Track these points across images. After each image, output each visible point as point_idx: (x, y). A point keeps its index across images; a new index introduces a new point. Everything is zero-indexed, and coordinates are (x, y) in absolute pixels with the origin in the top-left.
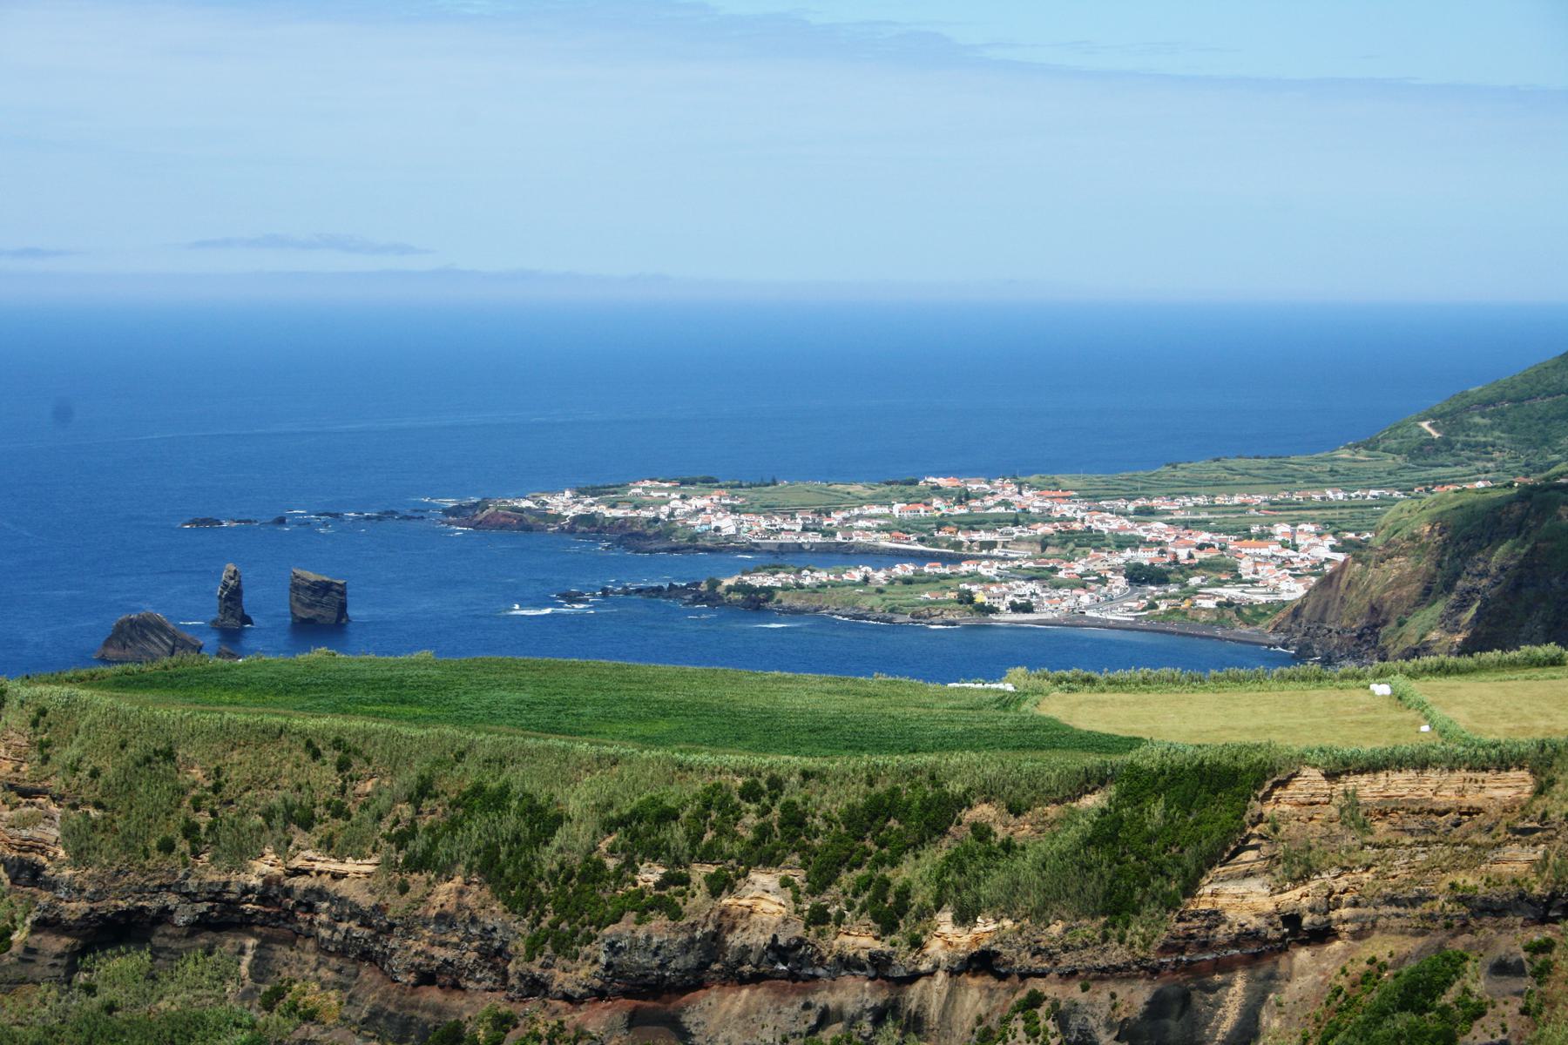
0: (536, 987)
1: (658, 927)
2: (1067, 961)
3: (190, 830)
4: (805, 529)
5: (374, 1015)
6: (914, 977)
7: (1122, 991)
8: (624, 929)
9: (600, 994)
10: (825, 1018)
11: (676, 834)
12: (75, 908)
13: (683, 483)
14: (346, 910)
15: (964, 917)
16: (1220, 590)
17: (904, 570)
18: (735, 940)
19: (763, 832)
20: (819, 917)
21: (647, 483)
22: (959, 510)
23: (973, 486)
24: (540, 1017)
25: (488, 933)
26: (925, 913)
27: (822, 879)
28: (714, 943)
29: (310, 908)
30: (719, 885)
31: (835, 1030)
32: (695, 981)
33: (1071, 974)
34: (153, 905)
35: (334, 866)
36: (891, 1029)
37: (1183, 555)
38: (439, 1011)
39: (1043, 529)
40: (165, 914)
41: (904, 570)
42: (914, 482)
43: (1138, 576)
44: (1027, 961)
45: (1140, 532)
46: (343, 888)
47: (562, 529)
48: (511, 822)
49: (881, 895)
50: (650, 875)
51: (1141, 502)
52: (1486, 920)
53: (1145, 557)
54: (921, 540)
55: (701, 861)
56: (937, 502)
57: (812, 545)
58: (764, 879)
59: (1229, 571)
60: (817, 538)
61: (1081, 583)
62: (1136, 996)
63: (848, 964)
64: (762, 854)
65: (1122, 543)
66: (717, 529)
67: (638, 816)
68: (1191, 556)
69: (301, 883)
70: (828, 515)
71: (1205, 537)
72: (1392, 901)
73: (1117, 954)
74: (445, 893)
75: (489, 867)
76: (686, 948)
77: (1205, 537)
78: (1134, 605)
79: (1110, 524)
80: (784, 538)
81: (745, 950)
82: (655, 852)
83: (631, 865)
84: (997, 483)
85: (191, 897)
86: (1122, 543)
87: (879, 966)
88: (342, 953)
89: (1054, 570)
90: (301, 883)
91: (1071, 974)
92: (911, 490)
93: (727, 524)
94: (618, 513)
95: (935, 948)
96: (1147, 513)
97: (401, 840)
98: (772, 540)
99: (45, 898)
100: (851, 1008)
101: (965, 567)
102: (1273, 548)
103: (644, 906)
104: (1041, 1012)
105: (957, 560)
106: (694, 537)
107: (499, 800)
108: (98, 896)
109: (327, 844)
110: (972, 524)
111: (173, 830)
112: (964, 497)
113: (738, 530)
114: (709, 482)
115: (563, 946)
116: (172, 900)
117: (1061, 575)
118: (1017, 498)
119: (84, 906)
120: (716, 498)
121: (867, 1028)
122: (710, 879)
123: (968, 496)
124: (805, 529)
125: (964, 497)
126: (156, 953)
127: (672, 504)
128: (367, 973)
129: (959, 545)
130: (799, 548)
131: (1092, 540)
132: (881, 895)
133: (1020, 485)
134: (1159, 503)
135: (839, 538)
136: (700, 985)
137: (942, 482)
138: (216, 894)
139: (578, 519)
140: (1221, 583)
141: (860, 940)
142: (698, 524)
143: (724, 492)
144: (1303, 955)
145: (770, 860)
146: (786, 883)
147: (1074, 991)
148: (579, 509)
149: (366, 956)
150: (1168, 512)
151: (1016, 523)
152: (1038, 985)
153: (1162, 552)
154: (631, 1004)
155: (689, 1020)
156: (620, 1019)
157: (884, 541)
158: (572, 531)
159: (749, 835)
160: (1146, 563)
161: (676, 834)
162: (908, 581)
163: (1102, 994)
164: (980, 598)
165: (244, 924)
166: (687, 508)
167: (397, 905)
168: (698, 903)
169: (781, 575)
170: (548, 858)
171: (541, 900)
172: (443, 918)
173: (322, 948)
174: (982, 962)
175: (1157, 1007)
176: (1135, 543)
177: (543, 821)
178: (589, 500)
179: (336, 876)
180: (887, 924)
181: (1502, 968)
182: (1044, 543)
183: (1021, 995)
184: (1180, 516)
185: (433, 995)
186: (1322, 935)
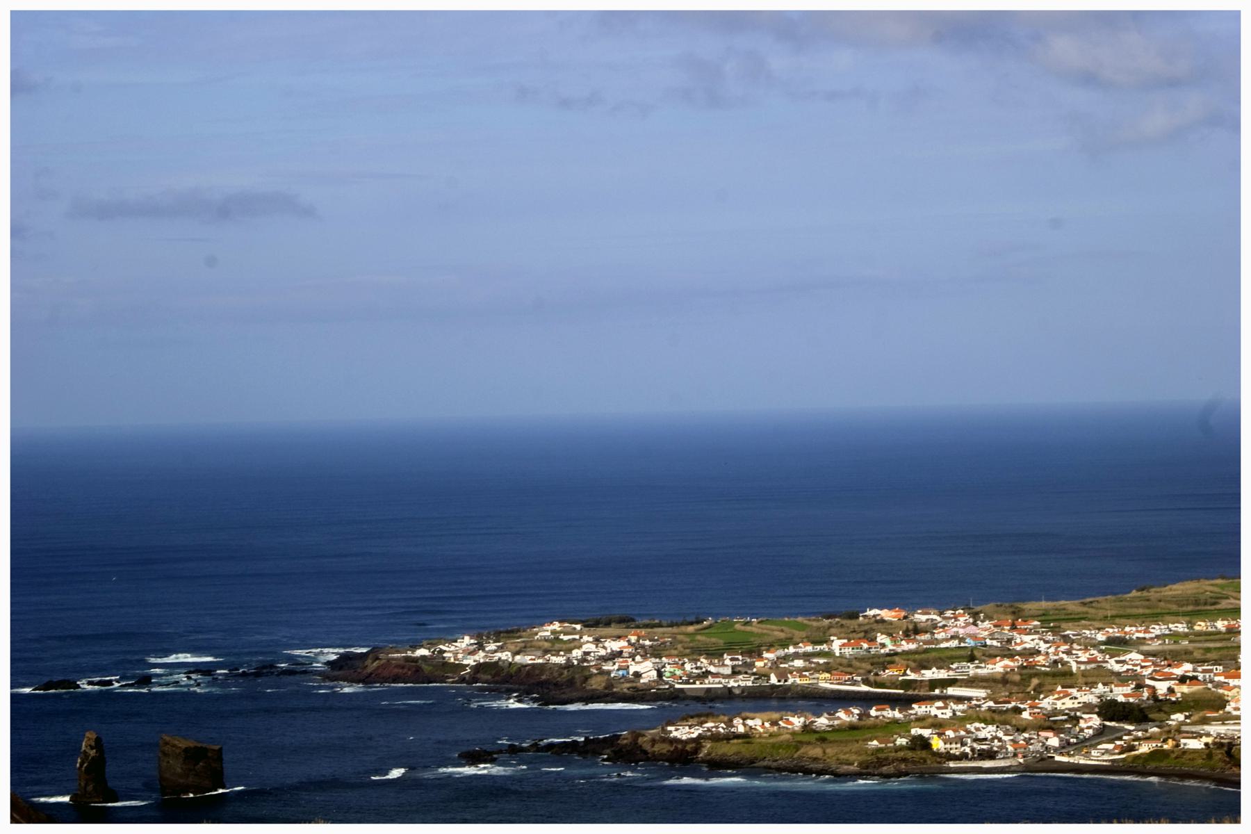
4: (735, 673)
13: (596, 624)
16: (1207, 728)
21: (556, 626)
22: (907, 646)
23: (920, 617)
37: (1162, 688)
42: (854, 616)
45: (1113, 665)
47: (463, 680)
51: (1113, 631)
54: (866, 682)
56: (881, 638)
57: (744, 689)
60: (745, 681)
66: (637, 675)
68: (1171, 690)
70: (760, 657)
71: (1187, 668)
77: (1187, 668)
78: (1111, 746)
80: (710, 683)
84: (949, 613)
89: (1018, 711)
92: (852, 624)
93: (646, 669)
94: (526, 659)
96: (1119, 645)
98: (698, 685)
101: (919, 709)
106: (610, 684)
110: (922, 660)
112: (913, 631)
113: (660, 674)
114: (626, 621)
117: (1025, 715)
118: (972, 629)
120: (633, 639)
123: (917, 630)
124: (735, 673)
125: (913, 631)
127: (586, 648)
129: (908, 684)
130: (728, 694)
131: (1061, 676)
133: (975, 615)
134: (1134, 632)
135: (774, 680)
137: (886, 614)
139: (479, 667)
140: (1205, 721)
143: (643, 632)
148: (480, 657)
150: (1141, 641)
151: (972, 659)
153: (1139, 686)
157: (826, 683)
158: (473, 678)
160: (1121, 699)
162: (852, 727)
166: (602, 652)
169: (710, 725)
178: (491, 646)
182: (1004, 680)
184: (1155, 646)
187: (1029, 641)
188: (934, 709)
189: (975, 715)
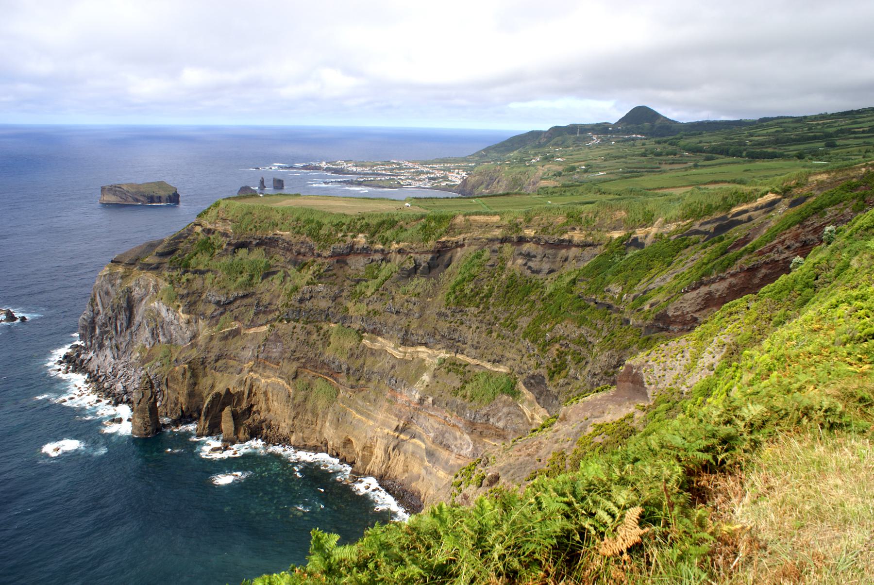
0: (319, 255)
1: (342, 245)
2: (416, 251)
3: (255, 227)
5: (290, 261)
6: (389, 253)
7: (426, 255)
8: (336, 245)
9: (332, 256)
10: (372, 261)
11: (345, 227)
12: (234, 242)
14: (284, 241)
15: (398, 243)
17: (387, 178)
18: (356, 247)
19: (362, 226)
20: (372, 242)
24: (320, 260)
25: (310, 246)
26: (391, 241)
27: (373, 235)
28: (352, 247)
29: (278, 241)
30: (354, 237)
31: (374, 263)
32: (348, 254)
33: (417, 253)
34: (249, 241)
35: (281, 233)
36: (384, 263)
38: (302, 260)
39: (413, 170)
40: (251, 242)
41: (387, 178)
43: (430, 179)
44: (409, 250)
46: (284, 237)
48: (314, 225)
49: (383, 239)
50: (340, 235)
52: (492, 242)
53: (432, 176)
55: (350, 232)
58: (361, 235)
59: (445, 178)
60: (371, 172)
61: (420, 180)
62: (430, 256)
63: (376, 251)
64: (361, 231)
65: (428, 173)
67: (337, 224)
69: (276, 236)
72: (475, 239)
73: (425, 249)
74: (302, 238)
75: (310, 234)
76: (347, 248)
79: (426, 170)
81: (358, 249)
82: (341, 231)
83: (337, 232)
85: (255, 239)
86: (428, 173)
87: (383, 250)
88: (284, 249)
90: (276, 236)
91: (417, 253)
93: (354, 169)
95: (393, 248)
97: (294, 228)
99: (228, 239)
100: (377, 259)
102: (455, 174)
103: (339, 241)
104: (412, 259)
105: (397, 176)
106: (348, 171)
107: (312, 221)
108: (238, 239)
109: (281, 230)
110: (400, 169)
111: (252, 227)
115: (324, 247)
116: (252, 240)
119: (236, 241)
121: (380, 262)
122: (352, 236)
126: (249, 249)
128: (288, 253)
131: (422, 172)
132: (383, 239)
136: (349, 255)
138: (260, 239)
141: (379, 246)
142: (349, 169)
144: (459, 249)
145: (362, 232)
146: (365, 236)
147: (417, 256)
149: (288, 250)
152: (412, 255)
154: (337, 258)
155: (348, 261)
156: (335, 261)
157: (384, 172)
159: (358, 227)
161: (345, 227)
163: (423, 256)
164: (402, 183)
165: (266, 244)
167: (294, 241)
168: (349, 239)
170: (322, 232)
171: (321, 239)
172: (302, 243)
173: (280, 248)
174: (400, 251)
175: (432, 259)
176: (430, 173)
177: (320, 225)
179: (282, 235)
180: (384, 244)
181: (494, 251)
182: (413, 172)
183: (409, 256)
185: (301, 257)
186: (462, 246)
187: (417, 167)
188: (402, 177)
189: (408, 178)
